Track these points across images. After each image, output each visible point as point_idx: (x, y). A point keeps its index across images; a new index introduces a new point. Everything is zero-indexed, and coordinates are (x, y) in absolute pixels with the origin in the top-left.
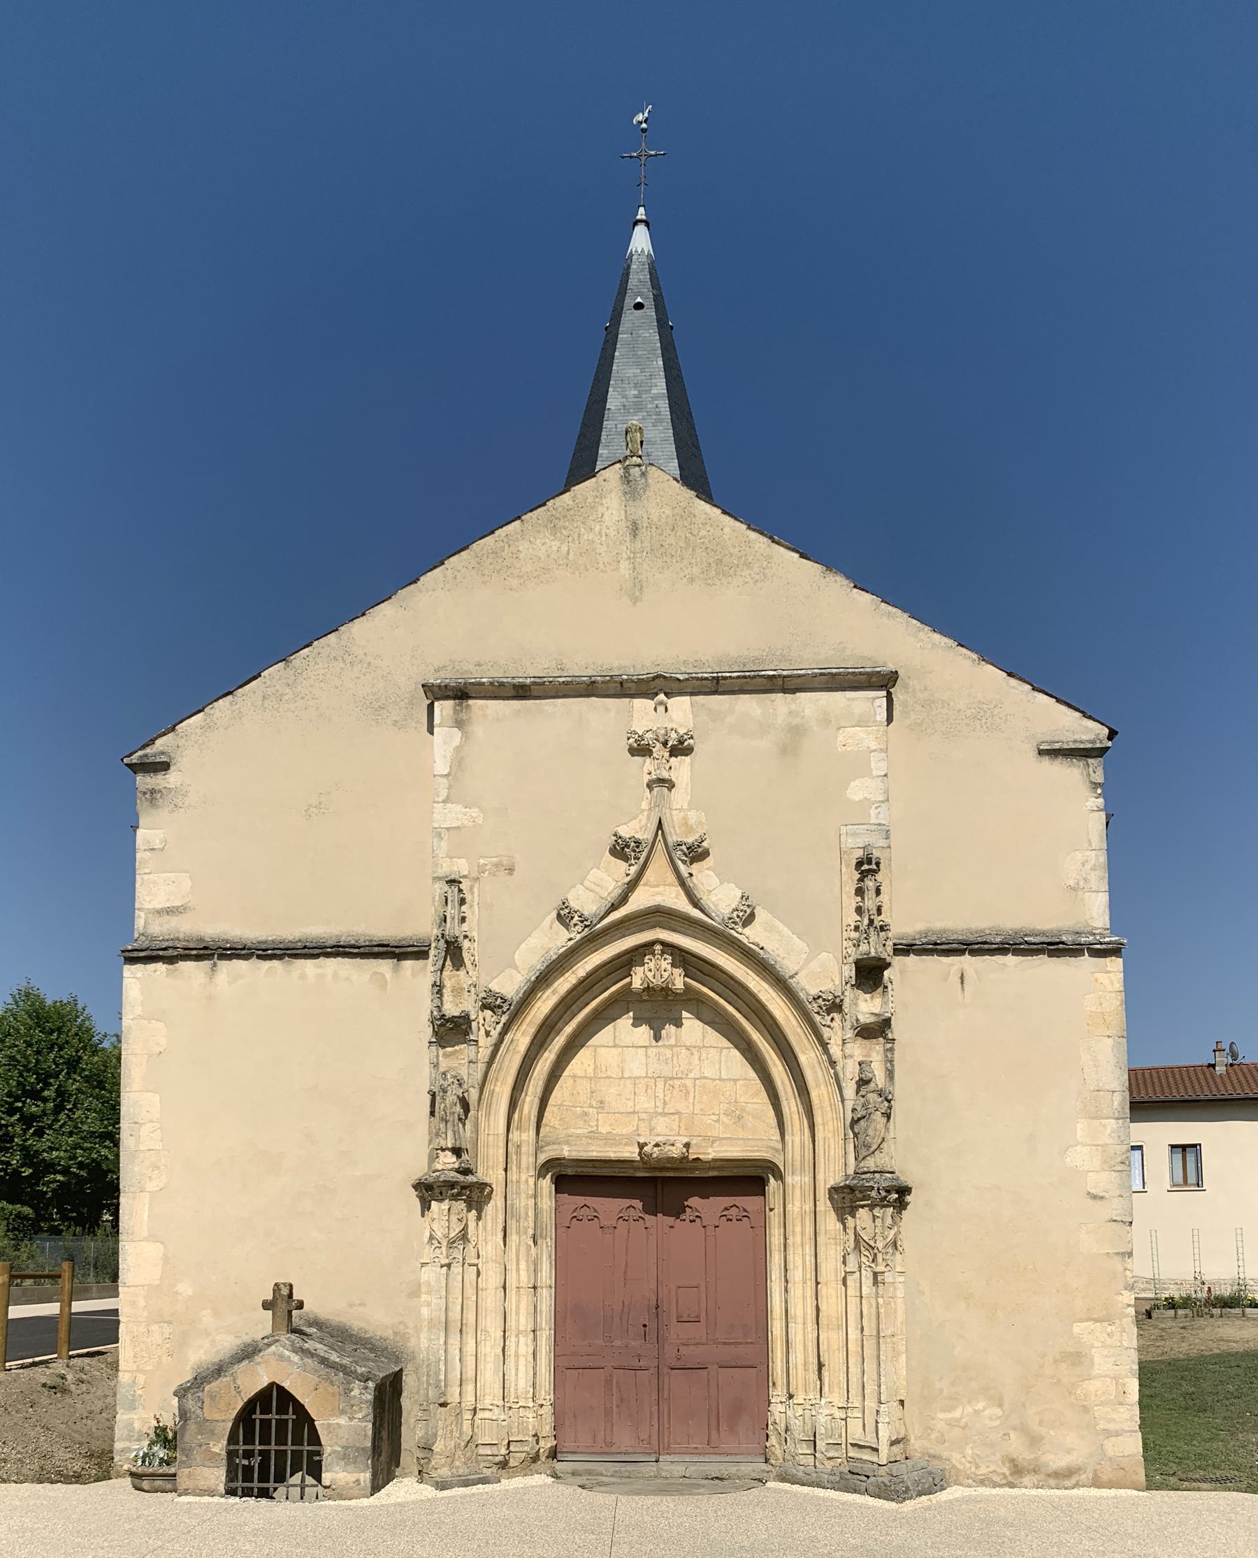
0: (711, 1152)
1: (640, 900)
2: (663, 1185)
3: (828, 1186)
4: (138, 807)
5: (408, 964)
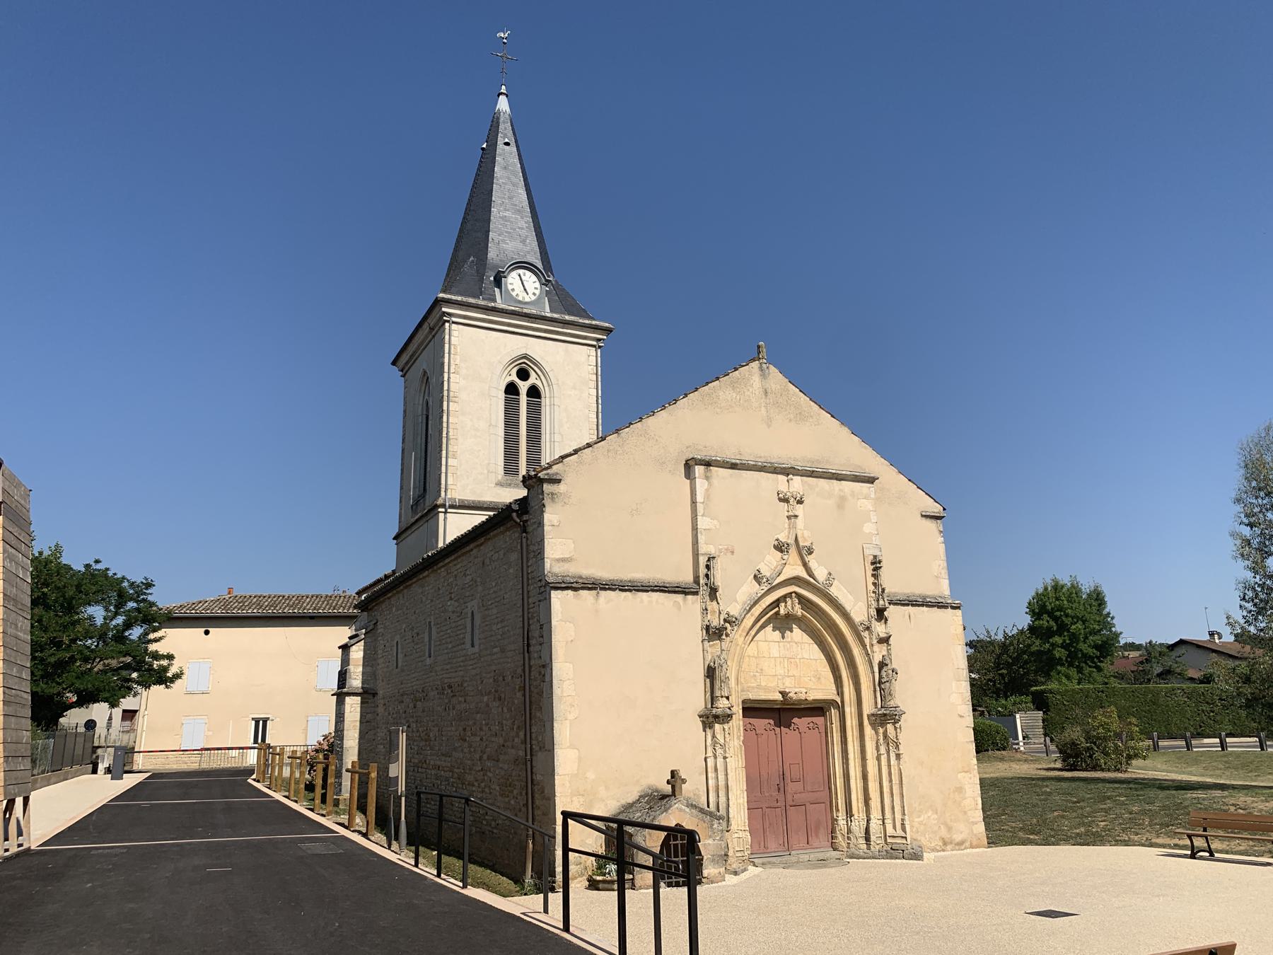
0: (811, 697)
1: (788, 573)
2: (780, 712)
4: (545, 502)
5: (689, 597)
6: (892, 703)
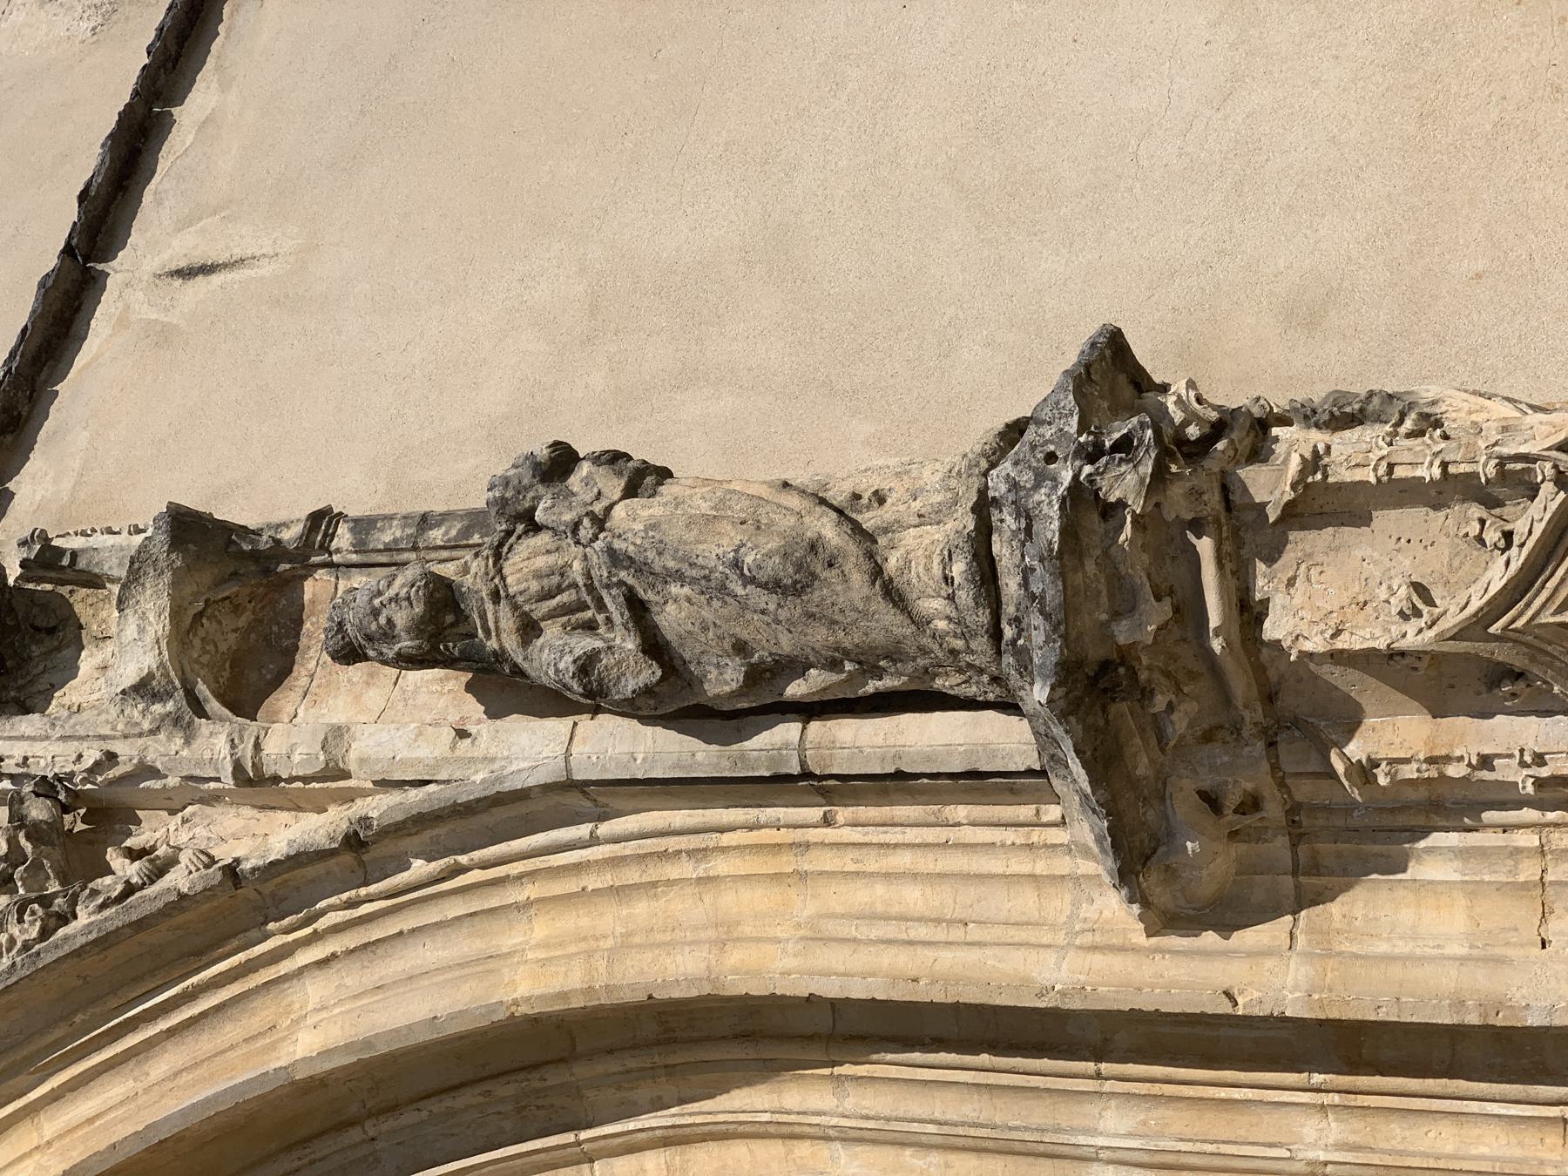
3: (1138, 936)
6: (925, 552)
